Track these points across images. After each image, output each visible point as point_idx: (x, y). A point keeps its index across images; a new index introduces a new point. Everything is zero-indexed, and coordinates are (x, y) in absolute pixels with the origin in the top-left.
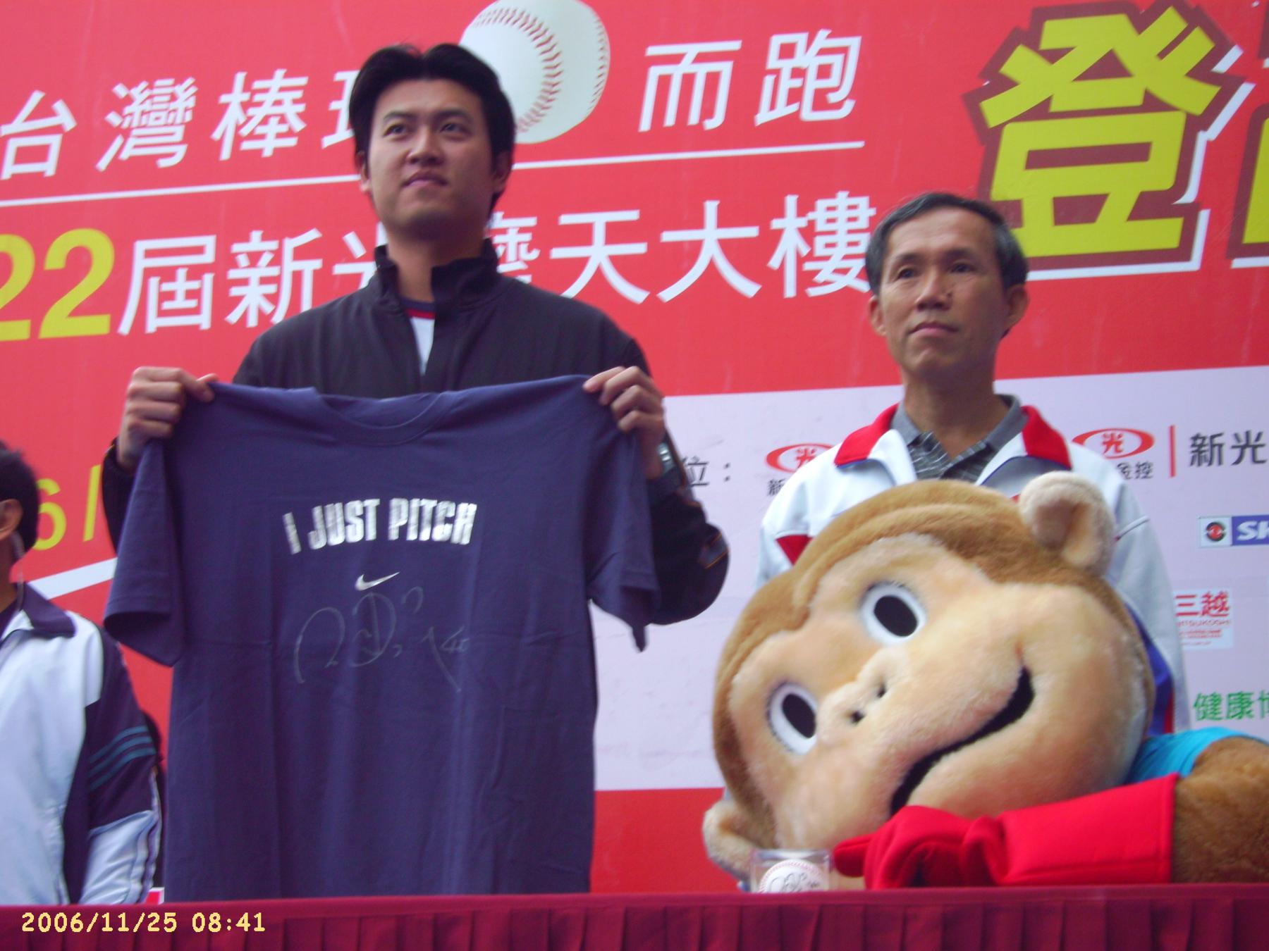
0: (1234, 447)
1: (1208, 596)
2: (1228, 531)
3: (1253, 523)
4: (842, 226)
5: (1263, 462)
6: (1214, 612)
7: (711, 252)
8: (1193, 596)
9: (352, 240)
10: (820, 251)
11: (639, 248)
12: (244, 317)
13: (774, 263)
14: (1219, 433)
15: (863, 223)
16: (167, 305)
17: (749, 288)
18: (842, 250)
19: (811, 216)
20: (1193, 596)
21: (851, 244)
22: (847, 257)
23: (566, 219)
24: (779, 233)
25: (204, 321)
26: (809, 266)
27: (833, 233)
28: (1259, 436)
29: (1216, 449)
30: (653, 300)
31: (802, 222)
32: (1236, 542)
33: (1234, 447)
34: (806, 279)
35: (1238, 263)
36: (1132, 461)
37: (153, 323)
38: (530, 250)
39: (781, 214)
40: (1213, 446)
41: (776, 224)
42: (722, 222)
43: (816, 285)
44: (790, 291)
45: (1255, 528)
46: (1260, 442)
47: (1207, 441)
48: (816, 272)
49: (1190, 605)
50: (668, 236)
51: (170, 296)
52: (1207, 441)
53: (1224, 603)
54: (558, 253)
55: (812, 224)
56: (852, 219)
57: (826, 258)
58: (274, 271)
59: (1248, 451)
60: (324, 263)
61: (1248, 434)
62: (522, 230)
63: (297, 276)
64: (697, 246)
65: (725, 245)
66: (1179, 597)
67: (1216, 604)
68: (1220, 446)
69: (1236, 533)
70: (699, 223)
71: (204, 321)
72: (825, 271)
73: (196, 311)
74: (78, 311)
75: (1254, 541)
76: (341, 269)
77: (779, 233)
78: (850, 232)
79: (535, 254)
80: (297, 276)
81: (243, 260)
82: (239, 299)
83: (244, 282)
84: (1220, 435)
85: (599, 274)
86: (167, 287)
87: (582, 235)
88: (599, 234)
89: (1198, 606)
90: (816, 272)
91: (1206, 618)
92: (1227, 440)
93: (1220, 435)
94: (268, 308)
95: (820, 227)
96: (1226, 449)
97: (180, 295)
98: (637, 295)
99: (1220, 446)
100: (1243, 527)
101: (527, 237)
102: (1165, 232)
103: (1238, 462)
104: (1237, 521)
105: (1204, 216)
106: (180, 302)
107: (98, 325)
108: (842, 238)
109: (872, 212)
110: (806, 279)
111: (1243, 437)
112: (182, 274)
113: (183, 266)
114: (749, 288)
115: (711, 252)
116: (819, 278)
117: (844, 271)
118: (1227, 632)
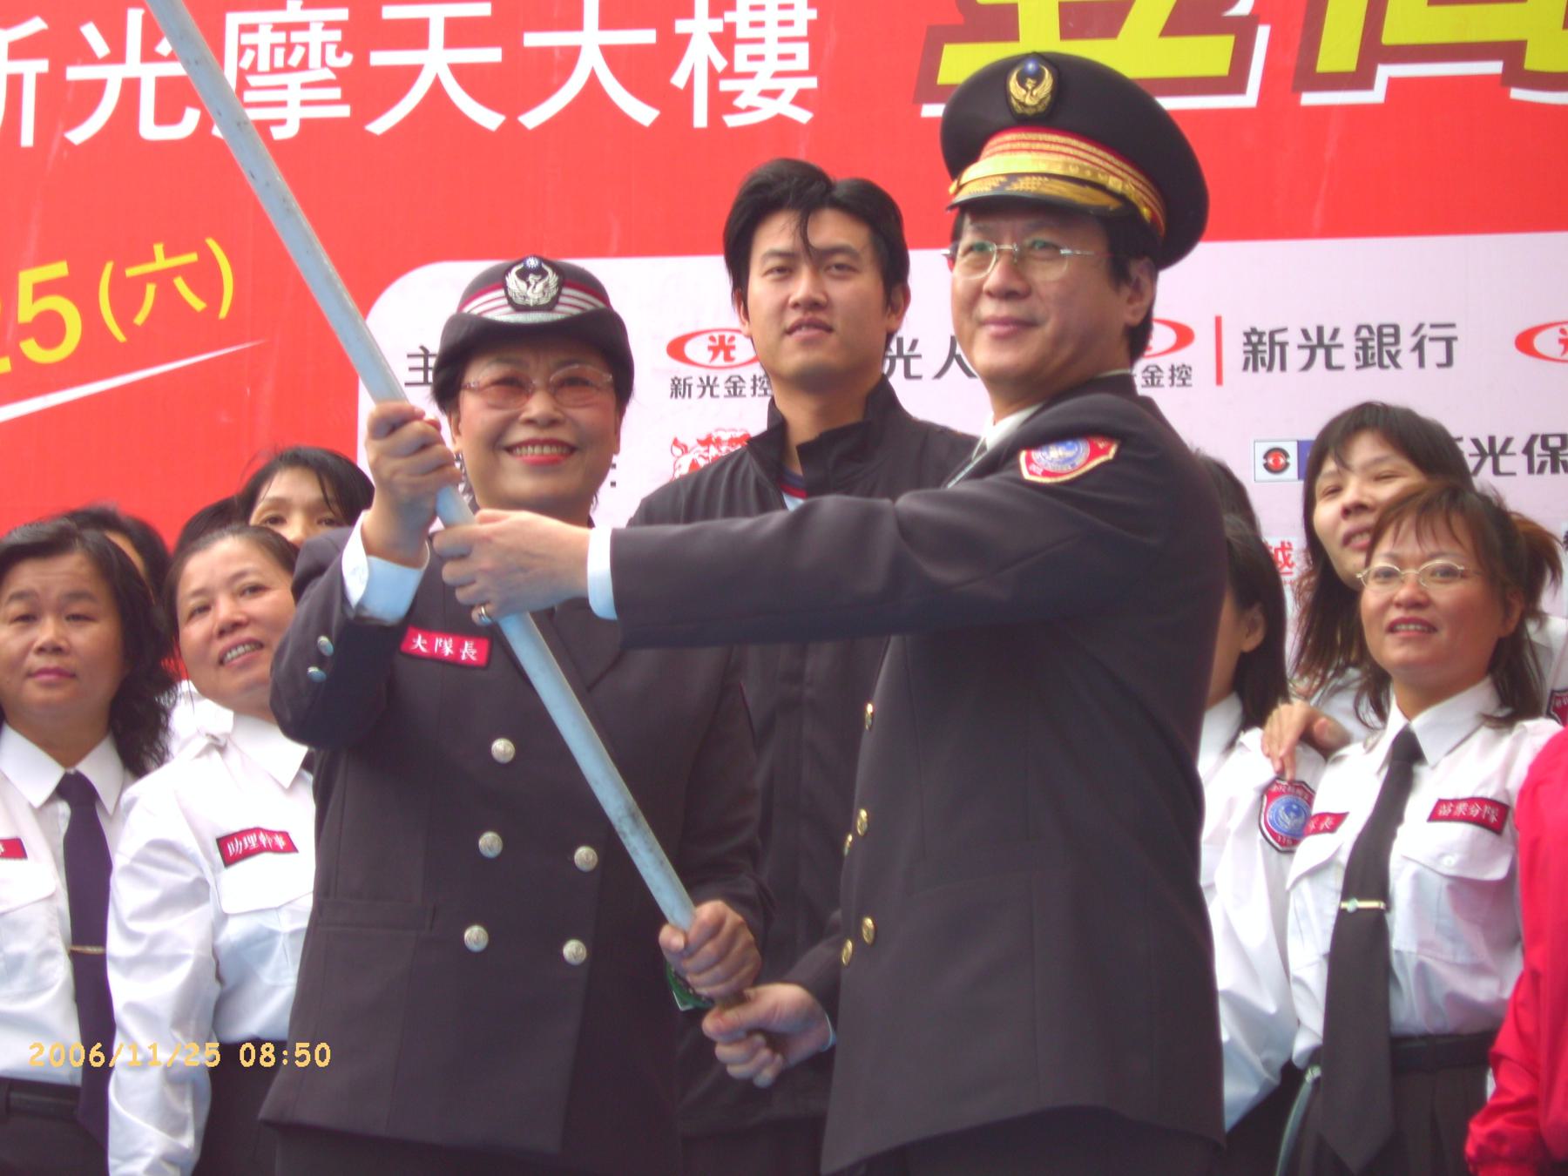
0: (1300, 347)
4: (771, 32)
5: (1341, 368)
7: (591, 61)
9: (91, 32)
10: (741, 65)
11: (493, 55)
13: (679, 80)
15: (801, 29)
17: (644, 114)
19: (729, 17)
21: (782, 57)
22: (778, 75)
23: (390, 12)
24: (686, 39)
26: (726, 85)
27: (761, 41)
28: (1336, 332)
29: (1277, 349)
30: (512, 126)
31: (717, 26)
33: (1300, 347)
34: (722, 103)
35: (1309, 99)
36: (1165, 363)
38: (339, 54)
39: (689, 14)
40: (1272, 343)
41: (681, 26)
42: (606, 23)
43: (737, 111)
44: (700, 119)
46: (1339, 340)
47: (1266, 339)
48: (736, 94)
50: (532, 40)
54: (379, 58)
55: (730, 28)
56: (789, 23)
57: (750, 75)
59: (1320, 353)
60: (51, 66)
61: (1320, 330)
62: (329, 26)
64: (573, 54)
65: (609, 53)
70: (576, 24)
72: (748, 93)
76: (75, 73)
77: (686, 39)
78: (782, 40)
79: (347, 59)
84: (1284, 330)
85: (437, 85)
87: (415, 34)
88: (437, 33)
90: (736, 94)
92: (1293, 338)
93: (1284, 330)
95: (743, 31)
96: (1291, 352)
98: (490, 120)
99: (1283, 345)
101: (336, 35)
102: (1210, 55)
105: (1263, 33)
108: (771, 49)
109: (813, 14)
110: (722, 103)
111: (1313, 335)
114: (644, 114)
115: (591, 61)
116: (740, 102)
117: (774, 94)
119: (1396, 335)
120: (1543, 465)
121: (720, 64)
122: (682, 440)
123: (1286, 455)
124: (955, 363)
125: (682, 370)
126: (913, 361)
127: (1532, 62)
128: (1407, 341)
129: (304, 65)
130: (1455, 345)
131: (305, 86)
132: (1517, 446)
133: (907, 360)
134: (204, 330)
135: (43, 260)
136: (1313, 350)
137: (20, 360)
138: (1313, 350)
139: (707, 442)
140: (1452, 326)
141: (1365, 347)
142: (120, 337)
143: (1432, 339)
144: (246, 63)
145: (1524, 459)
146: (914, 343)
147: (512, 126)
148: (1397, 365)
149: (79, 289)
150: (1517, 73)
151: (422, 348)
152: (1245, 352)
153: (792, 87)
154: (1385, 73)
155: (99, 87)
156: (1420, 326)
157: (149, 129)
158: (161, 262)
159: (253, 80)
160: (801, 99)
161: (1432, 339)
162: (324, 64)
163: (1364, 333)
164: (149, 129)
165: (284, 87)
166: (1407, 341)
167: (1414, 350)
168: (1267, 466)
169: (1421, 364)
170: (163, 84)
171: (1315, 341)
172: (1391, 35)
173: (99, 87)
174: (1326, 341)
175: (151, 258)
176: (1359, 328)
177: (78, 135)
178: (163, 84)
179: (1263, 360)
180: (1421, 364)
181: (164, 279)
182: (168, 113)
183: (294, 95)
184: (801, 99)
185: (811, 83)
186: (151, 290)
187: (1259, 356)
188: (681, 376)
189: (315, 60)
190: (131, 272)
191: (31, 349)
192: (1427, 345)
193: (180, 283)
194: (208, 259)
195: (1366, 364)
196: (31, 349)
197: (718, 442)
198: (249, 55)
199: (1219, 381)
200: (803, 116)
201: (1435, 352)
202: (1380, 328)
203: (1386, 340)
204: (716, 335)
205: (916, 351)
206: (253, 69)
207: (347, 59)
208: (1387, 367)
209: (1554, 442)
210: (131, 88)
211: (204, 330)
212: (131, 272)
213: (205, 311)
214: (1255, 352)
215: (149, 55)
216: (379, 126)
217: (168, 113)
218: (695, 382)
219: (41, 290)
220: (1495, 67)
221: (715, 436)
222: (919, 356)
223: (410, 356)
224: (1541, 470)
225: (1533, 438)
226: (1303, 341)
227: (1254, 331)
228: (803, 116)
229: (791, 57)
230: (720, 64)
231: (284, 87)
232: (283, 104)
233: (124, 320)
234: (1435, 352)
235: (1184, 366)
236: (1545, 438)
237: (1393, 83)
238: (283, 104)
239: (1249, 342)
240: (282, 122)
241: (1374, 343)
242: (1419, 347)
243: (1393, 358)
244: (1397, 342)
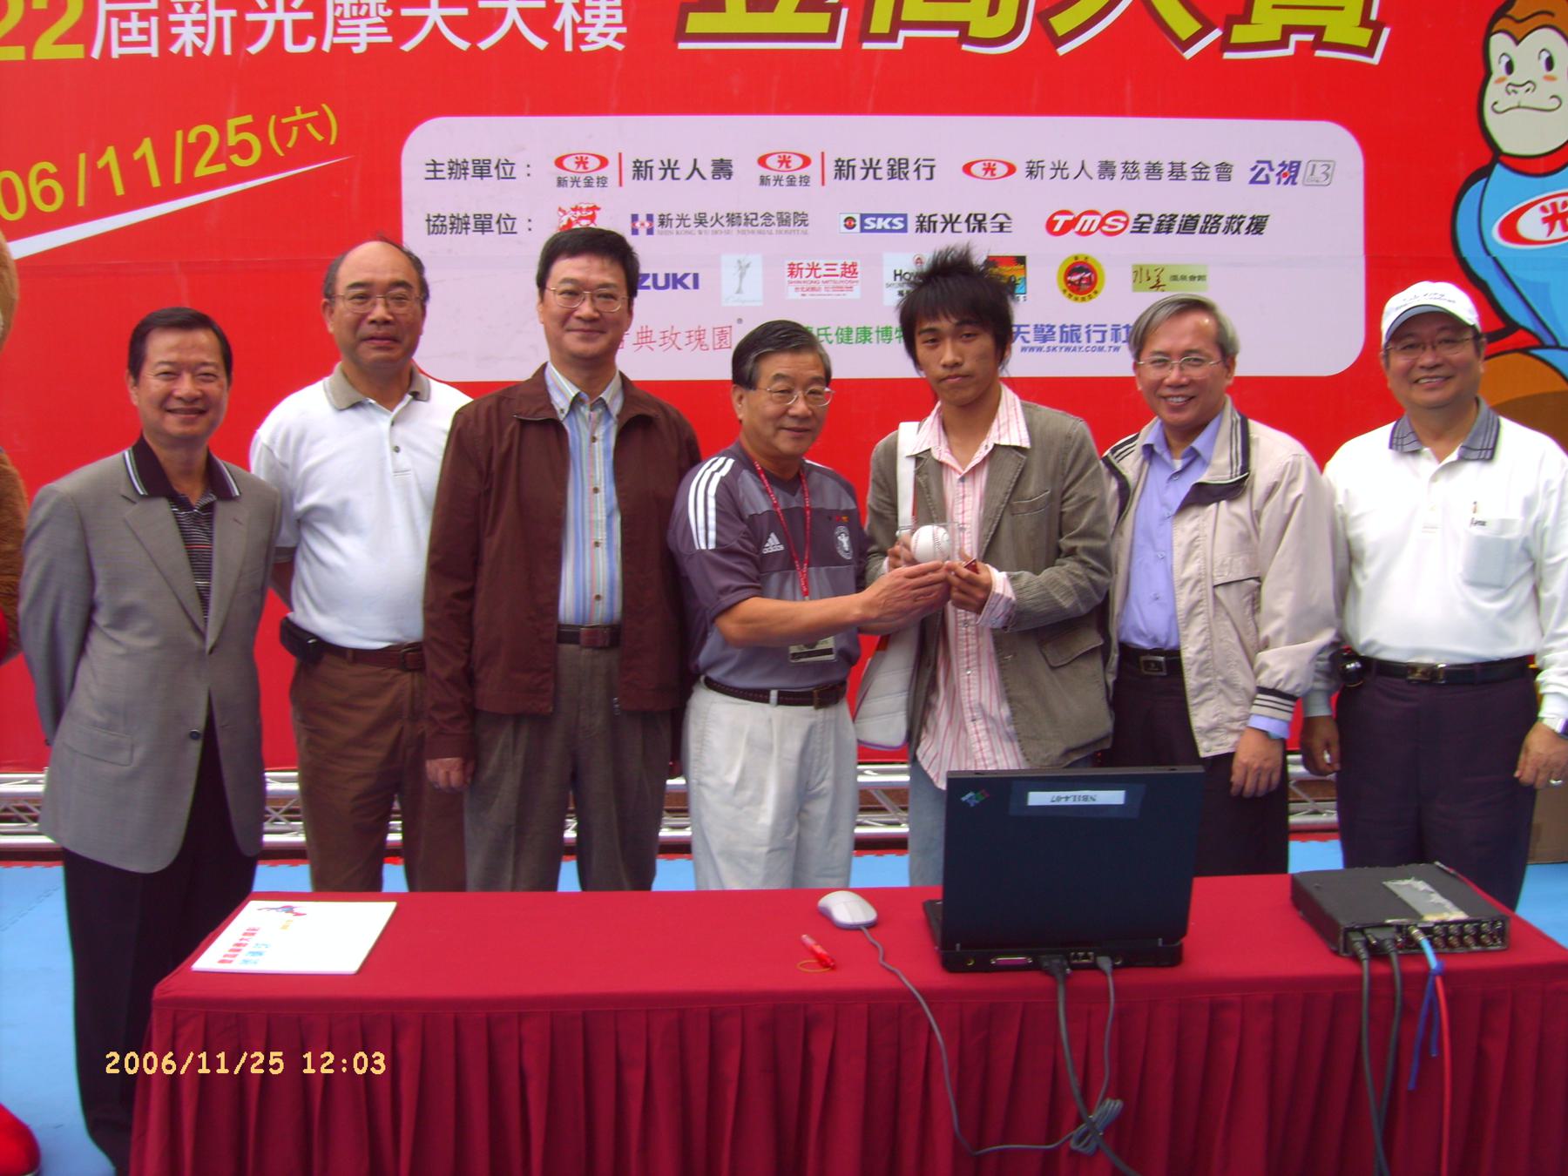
1: (845, 265)
2: (858, 223)
3: (874, 219)
5: (880, 179)
6: (848, 275)
8: (835, 264)
10: (588, 20)
12: (183, 49)
13: (557, 27)
16: (126, 39)
17: (540, 44)
18: (603, 20)
20: (835, 264)
21: (609, 17)
22: (607, 25)
25: (153, 51)
26: (581, 30)
28: (878, 161)
29: (851, 169)
30: (474, 49)
32: (863, 230)
33: (862, 168)
34: (579, 39)
35: (867, 46)
36: (797, 174)
37: (116, 52)
38: (385, 10)
43: (586, 43)
44: (569, 47)
45: (875, 222)
46: (879, 166)
48: (586, 35)
49: (834, 270)
51: (127, 32)
52: (845, 164)
53: (855, 270)
57: (593, 25)
58: (202, 17)
59: (871, 171)
63: (219, 21)
66: (827, 265)
67: (850, 270)
69: (863, 224)
71: (153, 51)
72: (592, 34)
73: (147, 44)
74: (62, 41)
75: (875, 230)
76: (251, 17)
79: (389, 13)
80: (219, 21)
81: (179, 8)
82: (177, 36)
83: (181, 24)
84: (854, 160)
85: (436, 28)
86: (125, 25)
89: (839, 271)
90: (586, 35)
91: (844, 279)
93: (854, 160)
94: (200, 43)
96: (856, 169)
97: (135, 32)
98: (463, 45)
100: (867, 221)
104: (863, 217)
105: (845, 12)
106: (135, 37)
107: (75, 51)
108: (603, 12)
110: (579, 39)
112: (134, 16)
113: (135, 11)
114: (540, 44)
116: (588, 39)
117: (605, 35)
118: (857, 288)
119: (907, 163)
120: (974, 228)
121: (578, 19)
122: (563, 208)
123: (855, 221)
124: (696, 173)
125: (563, 173)
126: (676, 171)
127: (973, 32)
128: (912, 167)
129: (367, 16)
130: (934, 169)
131: (369, 26)
132: (963, 219)
133: (673, 170)
134: (322, 151)
135: (239, 114)
136: (868, 169)
137: (231, 165)
138: (868, 169)
139: (575, 209)
140: (933, 160)
141: (892, 170)
142: (281, 153)
143: (924, 166)
144: (338, 14)
145: (966, 225)
146: (676, 162)
147: (474, 49)
148: (907, 179)
149: (258, 128)
150: (965, 38)
151: (433, 160)
153: (614, 32)
154: (903, 34)
155: (261, 25)
156: (918, 160)
157: (290, 47)
158: (300, 115)
159: (342, 23)
160: (619, 38)
161: (924, 166)
162: (378, 15)
163: (892, 162)
164: (290, 47)
165: (357, 26)
166: (912, 167)
167: (915, 171)
168: (845, 226)
169: (919, 178)
170: (296, 23)
172: (906, 16)
173: (261, 25)
174: (874, 166)
175: (294, 114)
176: (890, 160)
177: (254, 49)
178: (296, 23)
180: (919, 178)
181: (301, 124)
182: (299, 40)
183: (363, 30)
184: (619, 38)
185: (624, 30)
186: (295, 130)
188: (561, 176)
189: (373, 13)
190: (285, 120)
191: (236, 159)
192: (922, 169)
193: (310, 127)
194: (323, 114)
195: (892, 178)
196: (236, 159)
197: (581, 209)
198: (339, 9)
199: (823, 183)
200: (620, 47)
201: (925, 172)
202: (900, 160)
203: (902, 166)
204: (579, 156)
205: (678, 166)
206: (342, 17)
207: (389, 13)
208: (902, 179)
209: (980, 218)
210: (279, 25)
211: (322, 151)
212: (285, 120)
213: (323, 140)
215: (288, 9)
216: (407, 47)
217: (299, 40)
218: (569, 179)
219: (239, 129)
220: (955, 34)
221: (580, 206)
222: (678, 169)
223: (427, 164)
224: (973, 230)
225: (970, 215)
228: (620, 47)
229: (613, 16)
230: (578, 19)
231: (357, 26)
232: (357, 35)
233: (282, 145)
234: (925, 172)
236: (976, 215)
237: (907, 40)
238: (357, 35)
240: (357, 44)
241: (896, 167)
242: (917, 170)
243: (905, 174)
244: (907, 167)
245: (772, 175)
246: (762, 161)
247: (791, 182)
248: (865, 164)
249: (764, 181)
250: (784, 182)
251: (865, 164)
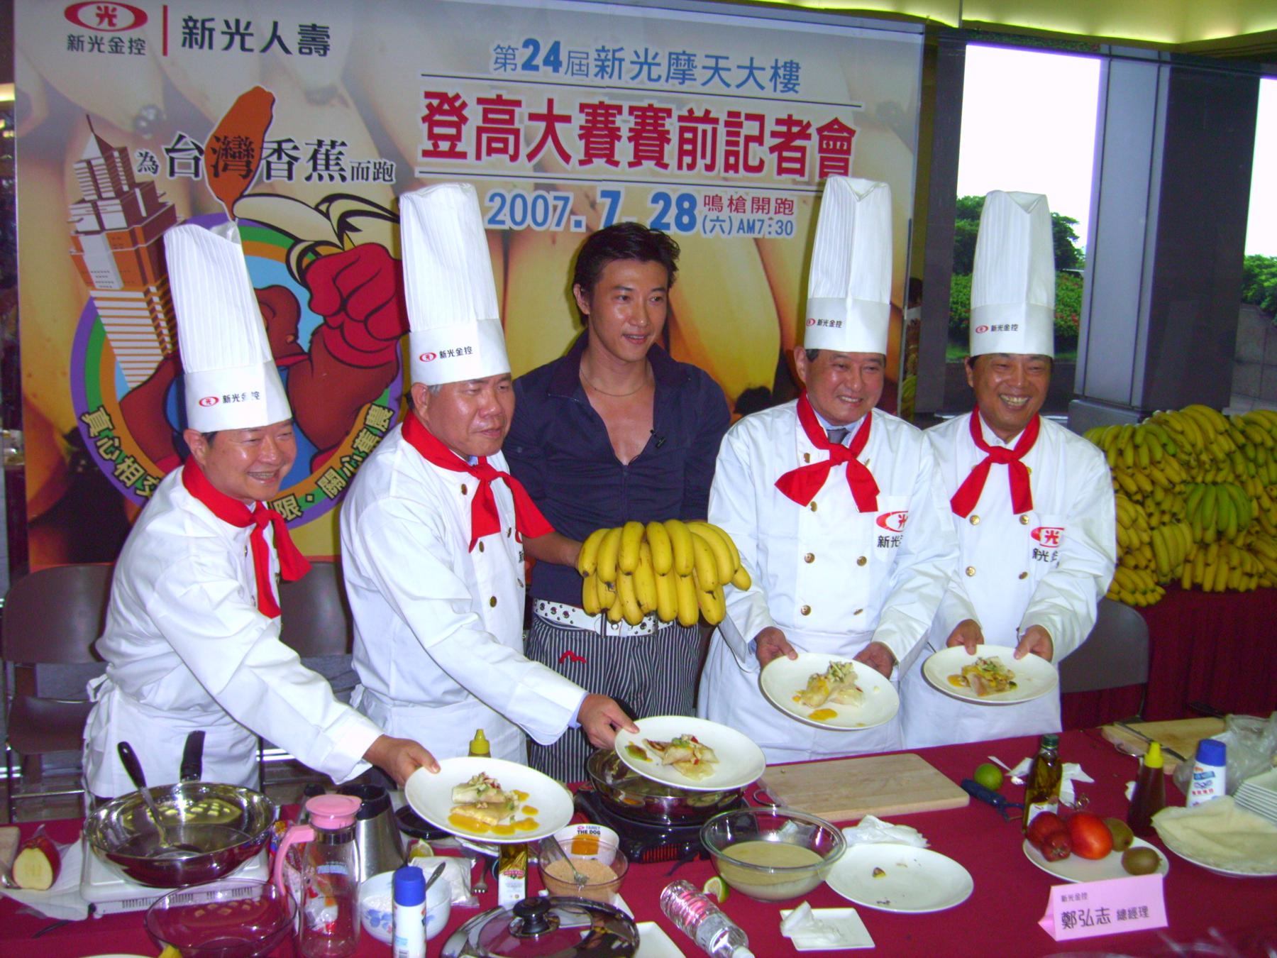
0: (223, 33)
5: (251, 50)
14: (210, 17)
28: (249, 24)
29: (207, 33)
33: (223, 33)
40: (204, 28)
46: (250, 31)
47: (199, 25)
59: (237, 39)
61: (238, 22)
68: (211, 30)
84: (212, 20)
93: (212, 20)
96: (216, 35)
99: (211, 30)
103: (228, 47)
136: (232, 36)
138: (232, 36)
152: (184, 33)
171: (234, 30)
174: (242, 30)
179: (196, 39)
187: (194, 36)
214: (191, 34)
226: (225, 29)
227: (190, 19)
235: (139, 40)
239: (187, 27)
245: (86, 34)
246: (72, 14)
247: (116, 47)
248: (228, 26)
249: (74, 43)
250: (106, 47)
251: (228, 26)
